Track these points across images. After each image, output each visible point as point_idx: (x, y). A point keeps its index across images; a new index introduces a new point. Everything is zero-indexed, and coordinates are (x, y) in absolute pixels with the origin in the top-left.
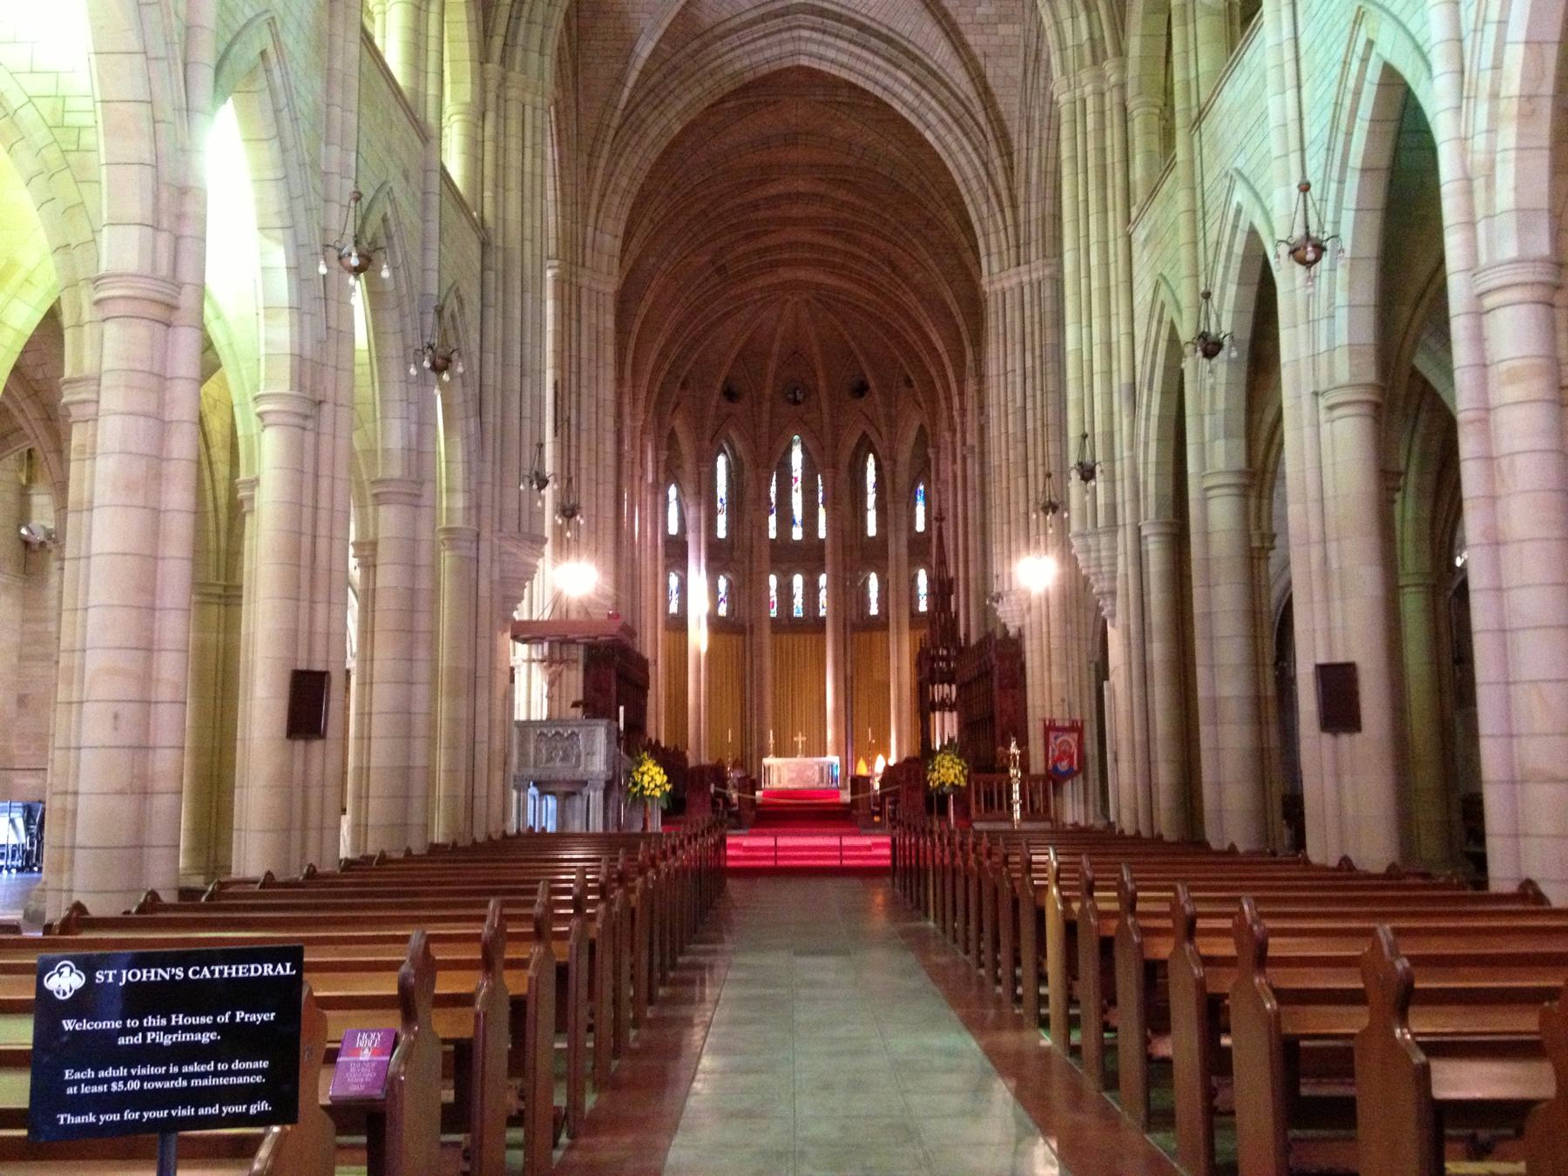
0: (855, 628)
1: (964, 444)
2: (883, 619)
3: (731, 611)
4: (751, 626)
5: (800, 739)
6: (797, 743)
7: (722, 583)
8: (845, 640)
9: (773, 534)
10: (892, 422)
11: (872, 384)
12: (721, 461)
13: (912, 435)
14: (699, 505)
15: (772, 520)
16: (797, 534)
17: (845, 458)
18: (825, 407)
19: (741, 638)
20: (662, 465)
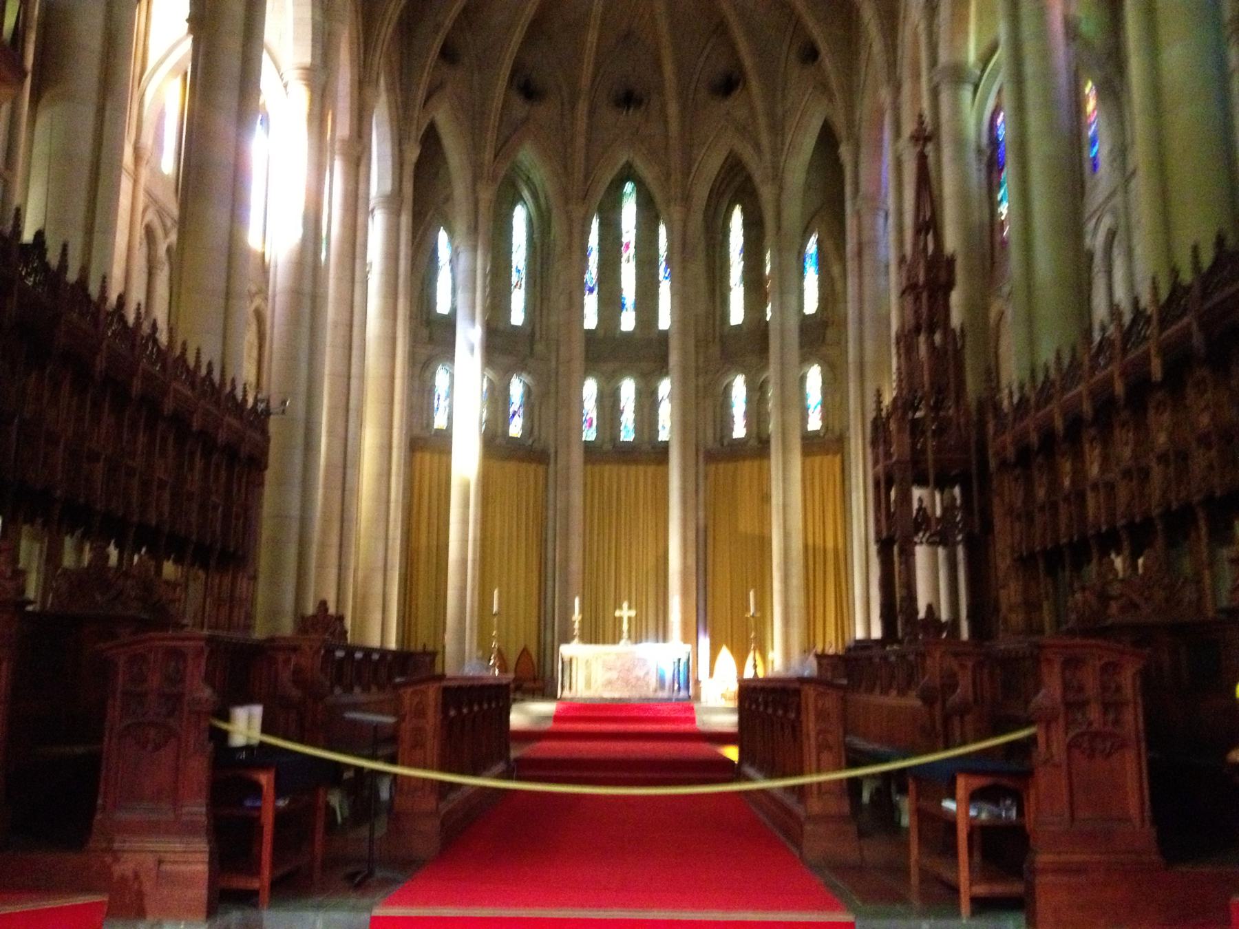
0: (711, 457)
1: (933, 62)
2: (753, 442)
3: (528, 429)
4: (556, 452)
5: (625, 613)
6: (621, 619)
7: (516, 389)
8: (697, 473)
9: (591, 321)
10: (777, 127)
11: (748, 62)
12: (520, 217)
13: (808, 142)
14: (474, 249)
15: (591, 304)
16: (628, 321)
17: (702, 192)
18: (673, 109)
19: (541, 469)
20: (409, 170)
